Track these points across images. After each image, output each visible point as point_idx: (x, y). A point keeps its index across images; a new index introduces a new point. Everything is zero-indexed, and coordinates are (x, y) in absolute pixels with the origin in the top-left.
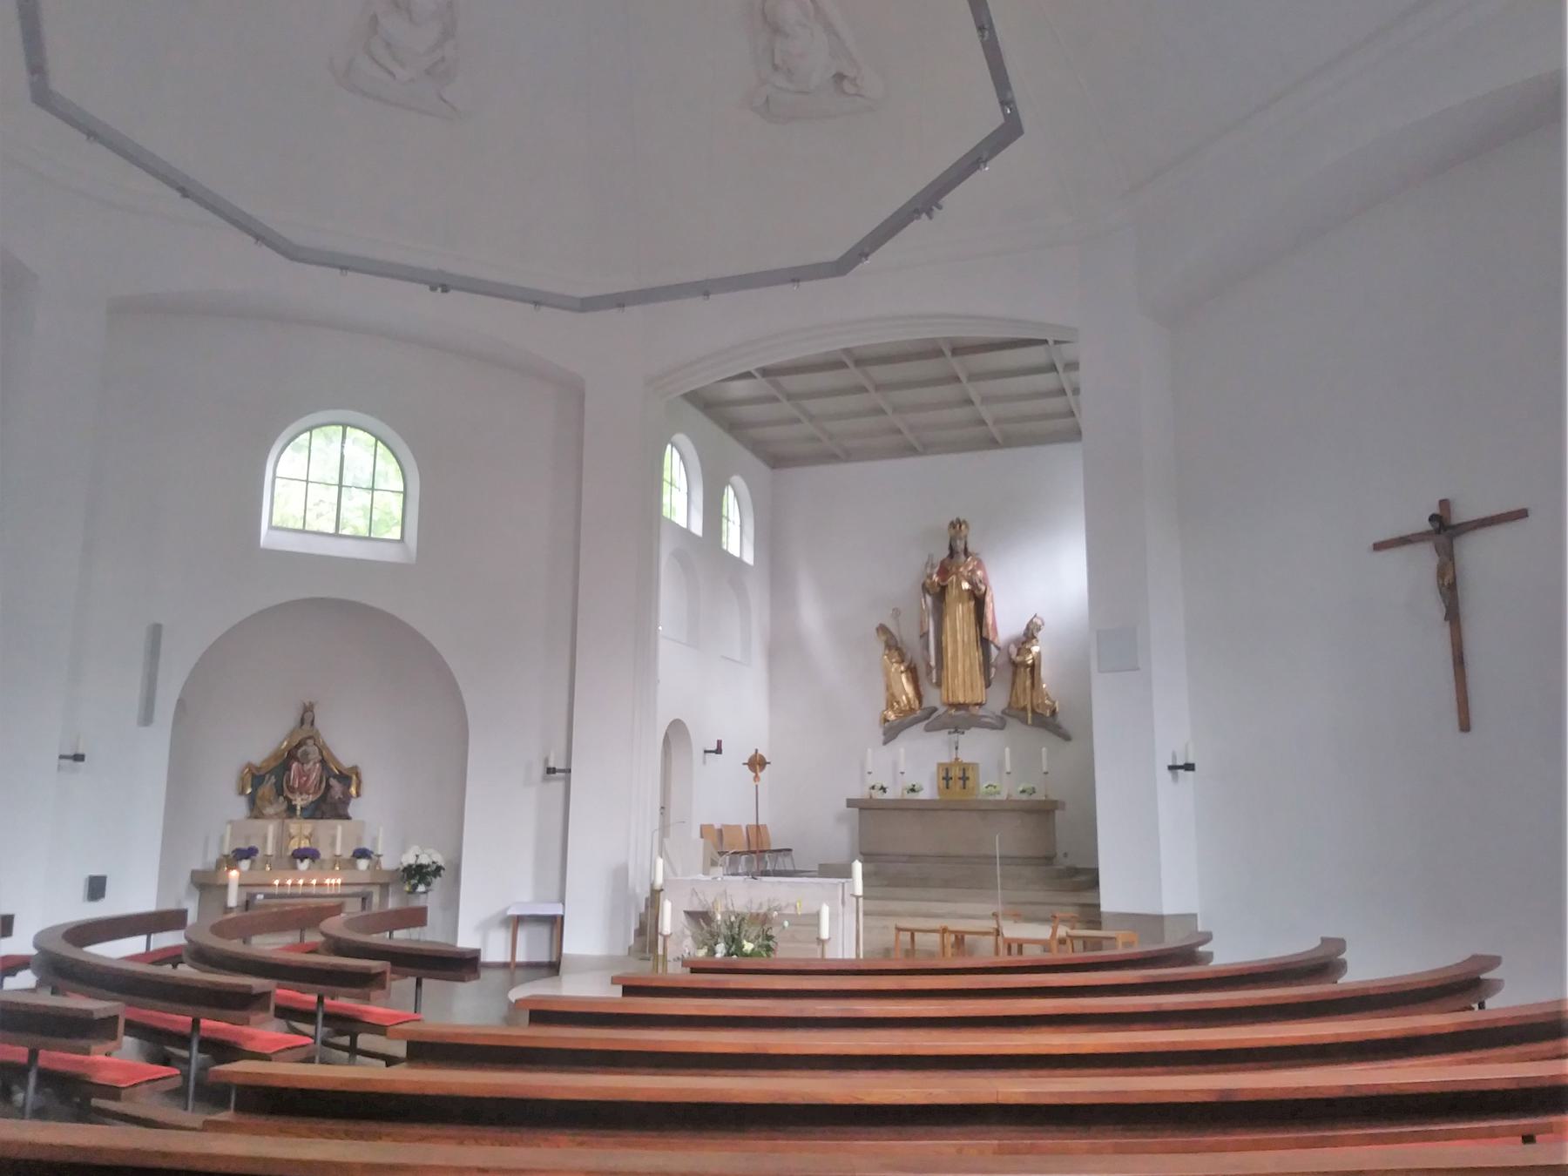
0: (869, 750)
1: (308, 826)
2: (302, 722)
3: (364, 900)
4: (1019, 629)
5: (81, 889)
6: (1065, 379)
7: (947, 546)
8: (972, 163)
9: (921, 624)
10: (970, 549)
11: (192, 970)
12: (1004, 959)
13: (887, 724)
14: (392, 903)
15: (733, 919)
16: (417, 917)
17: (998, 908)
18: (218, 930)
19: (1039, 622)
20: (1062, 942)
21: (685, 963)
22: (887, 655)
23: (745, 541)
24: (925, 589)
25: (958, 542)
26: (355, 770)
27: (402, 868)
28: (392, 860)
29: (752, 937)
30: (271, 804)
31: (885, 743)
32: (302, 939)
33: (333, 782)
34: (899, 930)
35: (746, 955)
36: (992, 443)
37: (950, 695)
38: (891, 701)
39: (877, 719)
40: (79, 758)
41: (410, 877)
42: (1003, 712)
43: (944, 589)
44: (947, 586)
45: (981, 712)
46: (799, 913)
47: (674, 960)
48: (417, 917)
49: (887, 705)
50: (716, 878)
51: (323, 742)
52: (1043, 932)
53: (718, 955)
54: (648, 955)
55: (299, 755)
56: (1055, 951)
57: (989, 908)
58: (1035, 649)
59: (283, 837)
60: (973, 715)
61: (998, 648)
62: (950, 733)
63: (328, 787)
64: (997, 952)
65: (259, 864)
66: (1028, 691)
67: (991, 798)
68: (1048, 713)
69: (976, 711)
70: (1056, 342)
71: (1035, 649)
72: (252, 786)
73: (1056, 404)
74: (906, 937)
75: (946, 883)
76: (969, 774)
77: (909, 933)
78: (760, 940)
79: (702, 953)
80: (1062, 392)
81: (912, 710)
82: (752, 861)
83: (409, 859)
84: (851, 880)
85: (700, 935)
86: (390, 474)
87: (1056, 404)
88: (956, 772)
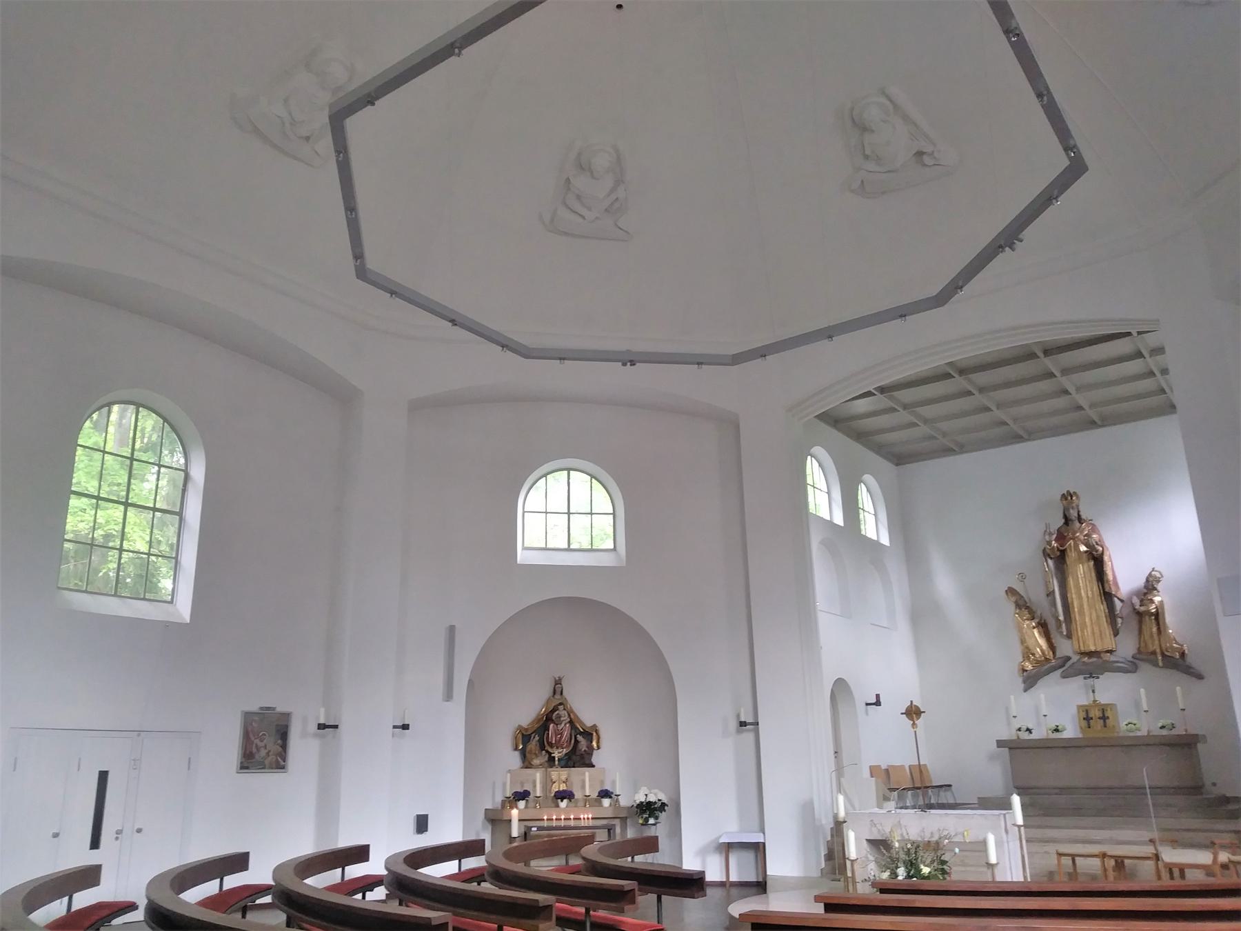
0: (1012, 697)
1: (564, 773)
2: (554, 693)
3: (609, 830)
4: (1139, 582)
5: (411, 825)
6: (1152, 363)
7: (1061, 515)
8: (1046, 200)
9: (1047, 584)
10: (1083, 517)
11: (494, 887)
12: (1166, 883)
13: (1025, 674)
14: (631, 834)
15: (909, 846)
16: (651, 845)
17: (1155, 835)
18: (508, 855)
19: (1158, 575)
20: (1225, 867)
21: (874, 885)
22: (1017, 614)
23: (880, 526)
24: (1046, 554)
25: (1071, 511)
26: (595, 728)
27: (635, 805)
28: (630, 796)
29: (928, 861)
30: (537, 756)
31: (1025, 691)
32: (567, 862)
33: (580, 738)
34: (1060, 855)
35: (924, 878)
36: (1092, 424)
37: (1081, 645)
38: (1027, 653)
39: (1015, 668)
40: (405, 727)
41: (643, 812)
44: (1065, 550)
45: (1113, 658)
46: (967, 841)
47: (862, 881)
48: (651, 845)
49: (1023, 657)
50: (890, 811)
51: (571, 707)
52: (1204, 857)
53: (900, 878)
54: (838, 877)
55: (554, 718)
56: (1219, 875)
57: (1146, 835)
58: (1157, 599)
59: (548, 782)
60: (1104, 661)
61: (1122, 601)
62: (1085, 678)
63: (577, 742)
64: (1159, 878)
65: (531, 804)
66: (1155, 636)
67: (1131, 734)
68: (1177, 655)
69: (1107, 657)
70: (1139, 333)
71: (1157, 599)
72: (523, 744)
73: (1146, 385)
74: (1067, 861)
75: (1100, 813)
76: (1108, 714)
77: (1070, 858)
78: (935, 864)
79: (886, 875)
80: (1151, 374)
81: (1047, 660)
82: (918, 796)
83: (640, 798)
84: (1011, 811)
85: (884, 860)
86: (603, 501)
87: (1146, 385)
88: (1095, 713)
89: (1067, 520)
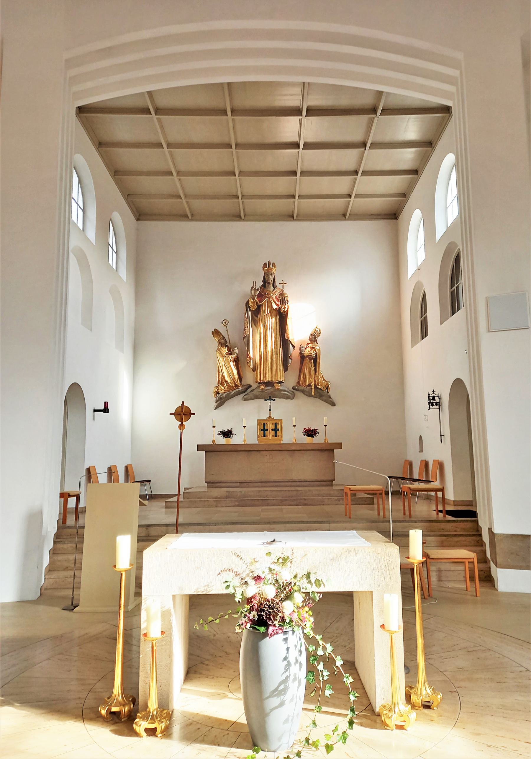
13: (218, 396)
25: (270, 277)
38: (222, 381)
42: (293, 388)
43: (259, 307)
69: (277, 386)
81: (236, 386)
88: (271, 426)
89: (265, 282)
